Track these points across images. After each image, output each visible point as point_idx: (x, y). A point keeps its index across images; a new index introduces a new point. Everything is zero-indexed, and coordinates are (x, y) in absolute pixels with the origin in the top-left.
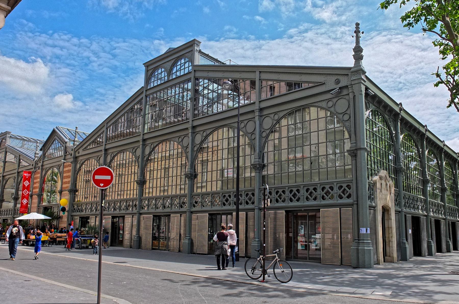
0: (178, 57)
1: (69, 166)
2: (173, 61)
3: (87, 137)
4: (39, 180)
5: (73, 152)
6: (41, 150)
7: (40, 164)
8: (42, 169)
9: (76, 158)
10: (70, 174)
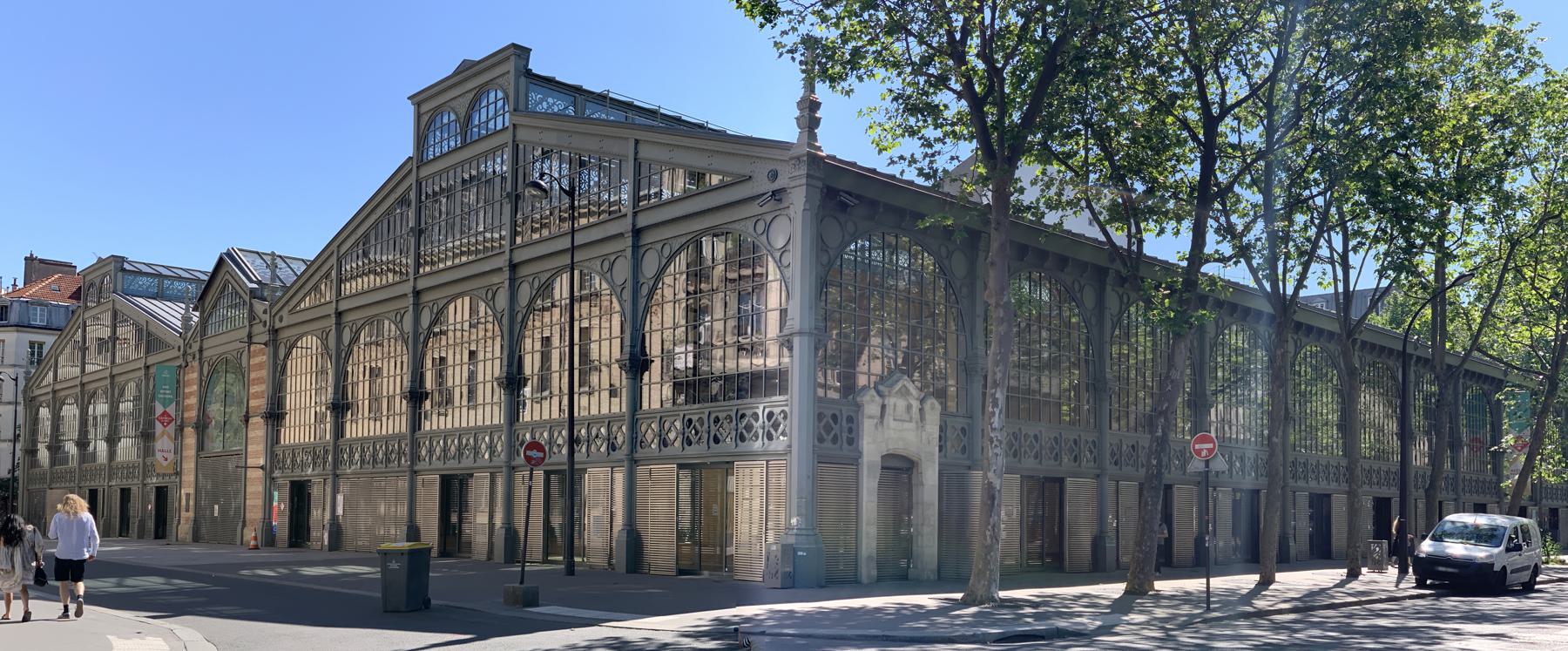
0: (481, 87)
1: (261, 352)
2: (471, 96)
3: (299, 277)
4: (195, 388)
5: (266, 317)
7: (196, 347)
8: (200, 359)
9: (275, 332)
10: (264, 373)
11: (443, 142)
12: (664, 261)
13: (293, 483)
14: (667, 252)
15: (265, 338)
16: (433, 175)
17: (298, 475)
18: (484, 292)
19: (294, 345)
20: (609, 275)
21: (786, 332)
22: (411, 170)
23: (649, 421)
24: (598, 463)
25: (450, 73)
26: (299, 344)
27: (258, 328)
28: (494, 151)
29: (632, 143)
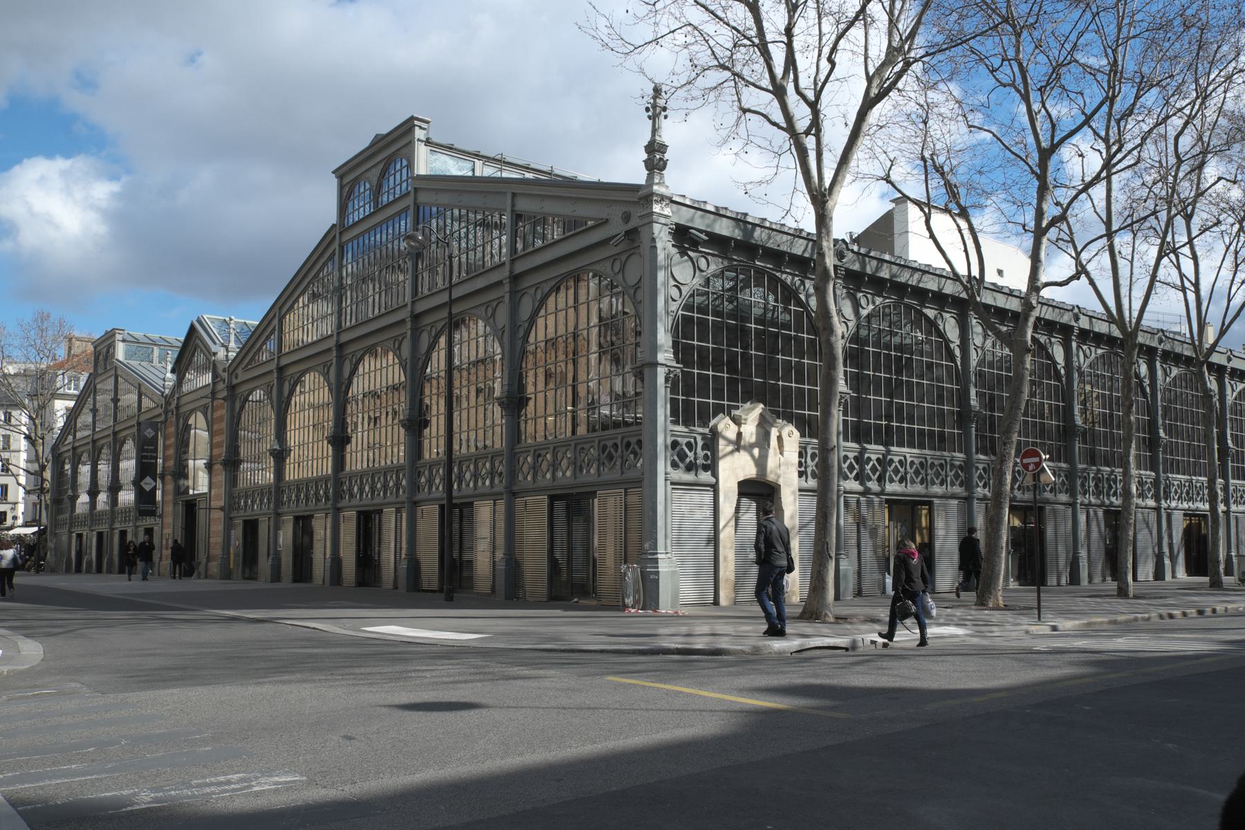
2: (381, 166)
5: (225, 375)
6: (173, 371)
8: (177, 415)
9: (232, 388)
11: (361, 208)
12: (537, 304)
13: (246, 522)
14: (539, 296)
15: (225, 394)
16: (351, 240)
17: (249, 514)
18: (392, 343)
19: (246, 400)
20: (492, 320)
21: (639, 364)
22: (335, 236)
23: (525, 455)
24: (484, 496)
25: (367, 144)
26: (250, 398)
27: (221, 386)
28: (399, 214)
29: (509, 197)
